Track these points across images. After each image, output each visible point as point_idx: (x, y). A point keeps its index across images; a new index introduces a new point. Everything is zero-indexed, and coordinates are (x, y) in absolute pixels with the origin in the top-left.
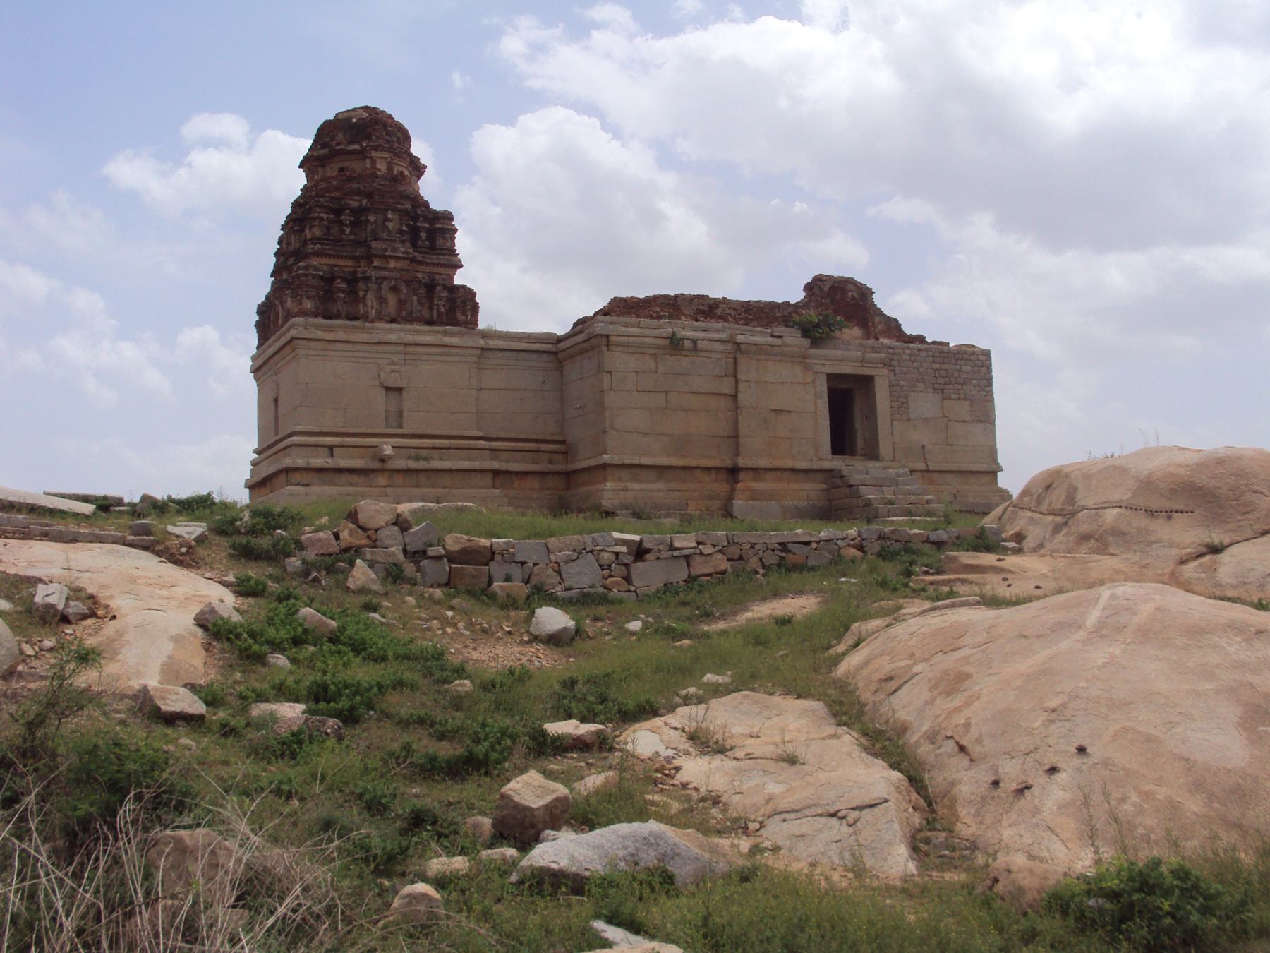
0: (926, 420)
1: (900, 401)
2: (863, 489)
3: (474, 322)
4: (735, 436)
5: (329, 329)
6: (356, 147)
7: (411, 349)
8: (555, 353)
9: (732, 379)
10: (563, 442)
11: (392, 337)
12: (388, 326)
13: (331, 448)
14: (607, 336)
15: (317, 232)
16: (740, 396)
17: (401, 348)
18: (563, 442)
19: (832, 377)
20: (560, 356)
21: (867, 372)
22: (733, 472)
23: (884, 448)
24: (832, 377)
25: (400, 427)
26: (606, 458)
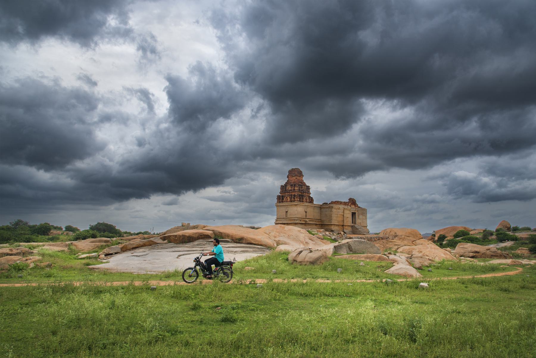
0: (361, 219)
1: (358, 216)
2: (359, 229)
3: (313, 203)
4: (343, 221)
5: (300, 203)
6: (299, 175)
8: (320, 207)
10: (321, 220)
11: (306, 205)
13: (301, 220)
18: (321, 220)
19: (352, 213)
21: (355, 212)
22: (343, 225)
23: (357, 223)
24: (352, 213)
25: (306, 217)
26: (332, 223)
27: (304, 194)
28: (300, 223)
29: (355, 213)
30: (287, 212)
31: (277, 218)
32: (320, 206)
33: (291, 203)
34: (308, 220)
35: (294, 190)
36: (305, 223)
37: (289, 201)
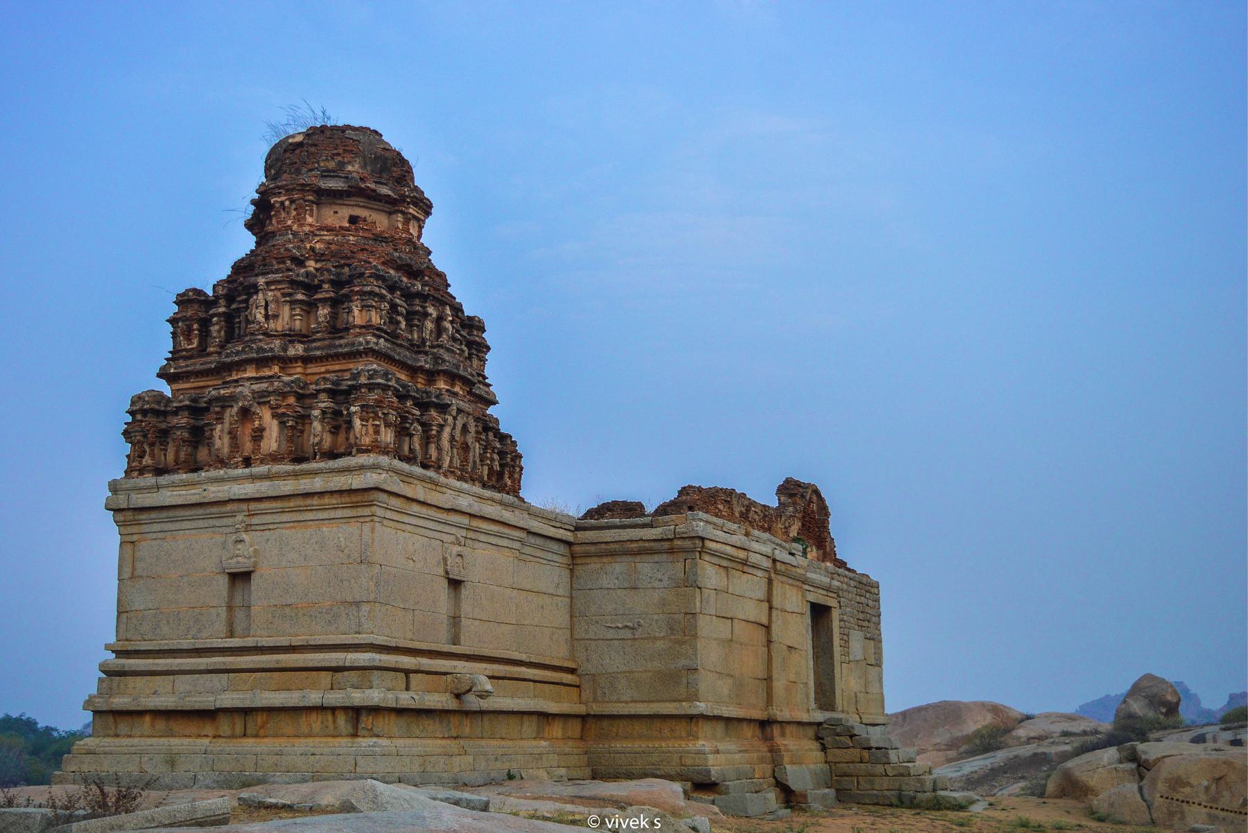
4: (769, 679)
5: (407, 477)
6: (384, 190)
7: (476, 523)
8: (569, 544)
9: (766, 604)
10: (572, 671)
11: (464, 503)
12: (458, 484)
13: (407, 672)
14: (703, 539)
15: (376, 319)
16: (774, 628)
17: (465, 520)
18: (572, 671)
20: (577, 549)
22: (765, 724)
25: (455, 641)
27: (442, 385)
28: (400, 712)
29: (829, 608)
30: (240, 578)
31: (120, 653)
32: (568, 536)
33: (296, 475)
34: (480, 674)
35: (336, 329)
36: (452, 704)
37: (274, 458)
